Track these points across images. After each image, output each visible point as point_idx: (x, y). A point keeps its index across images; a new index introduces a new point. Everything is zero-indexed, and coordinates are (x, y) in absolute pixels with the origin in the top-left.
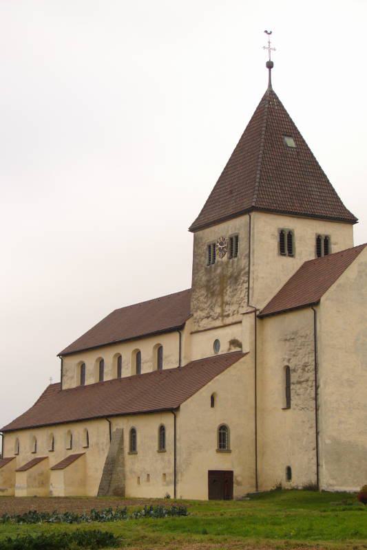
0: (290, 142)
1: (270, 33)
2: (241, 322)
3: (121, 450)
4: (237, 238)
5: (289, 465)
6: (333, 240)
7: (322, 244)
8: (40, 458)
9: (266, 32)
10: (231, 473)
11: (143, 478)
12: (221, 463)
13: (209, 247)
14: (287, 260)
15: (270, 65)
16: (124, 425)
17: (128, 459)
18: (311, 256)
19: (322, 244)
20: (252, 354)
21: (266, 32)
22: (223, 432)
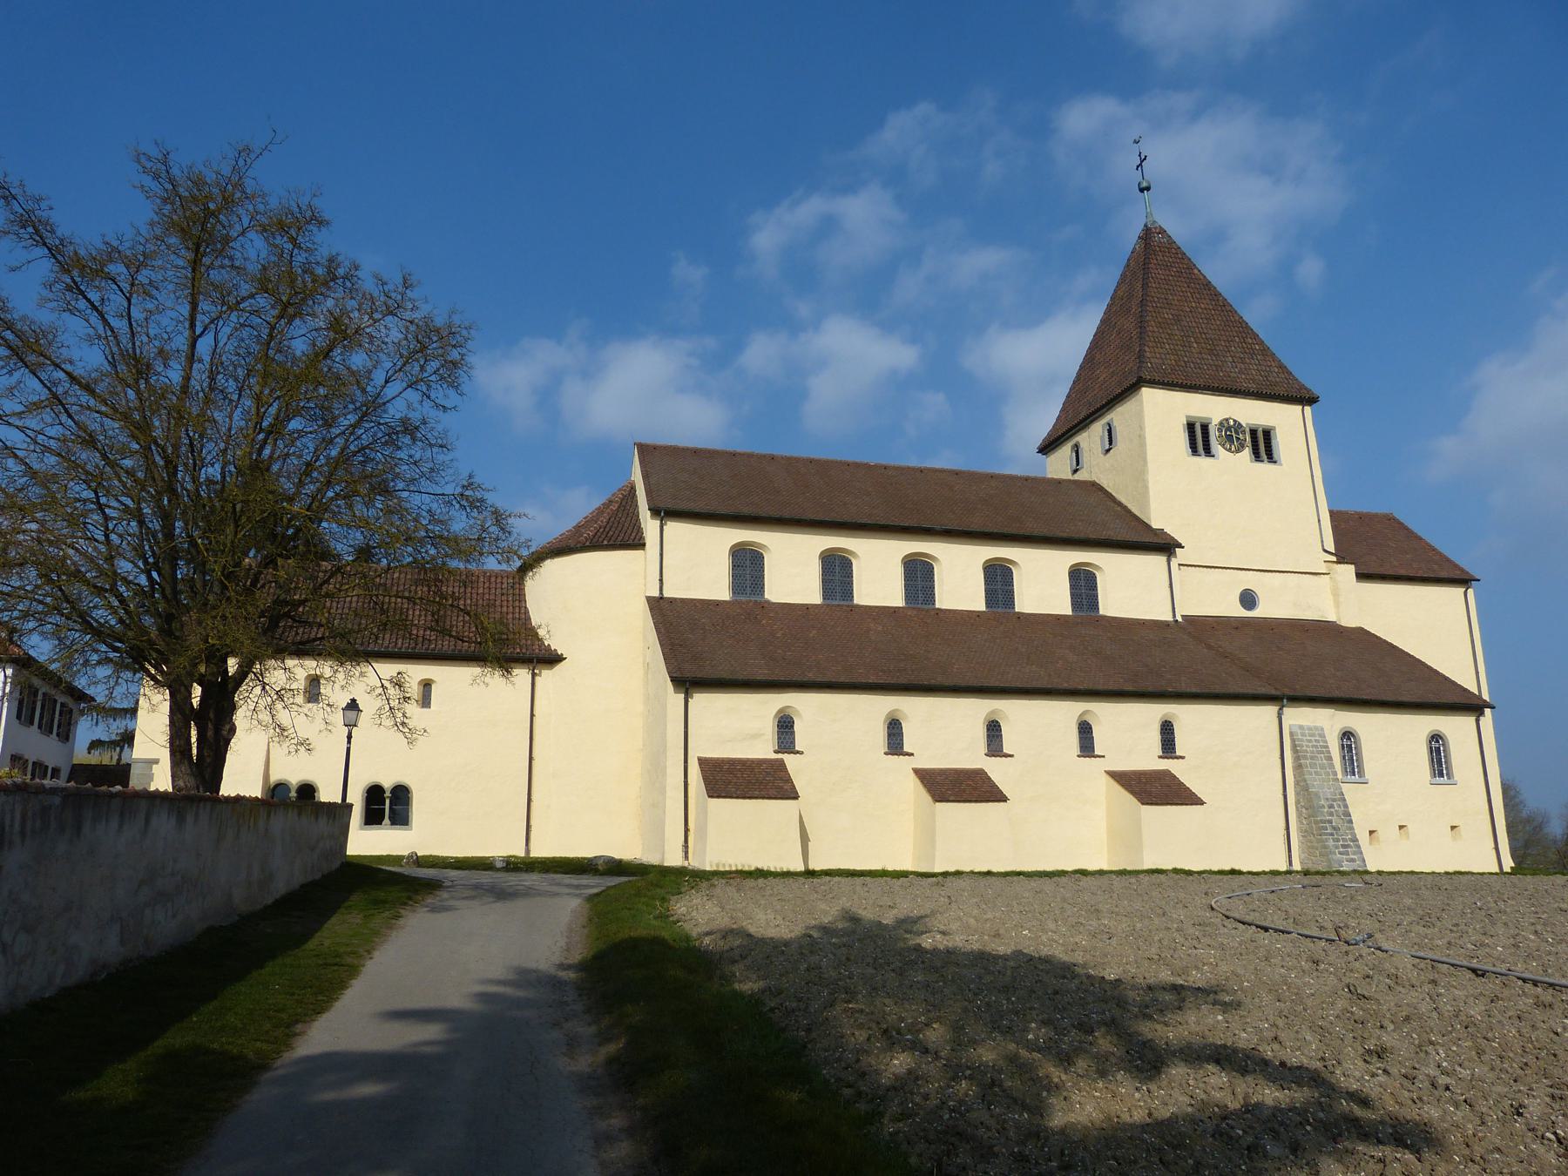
4: (1267, 434)
13: (1190, 427)
16: (1328, 722)
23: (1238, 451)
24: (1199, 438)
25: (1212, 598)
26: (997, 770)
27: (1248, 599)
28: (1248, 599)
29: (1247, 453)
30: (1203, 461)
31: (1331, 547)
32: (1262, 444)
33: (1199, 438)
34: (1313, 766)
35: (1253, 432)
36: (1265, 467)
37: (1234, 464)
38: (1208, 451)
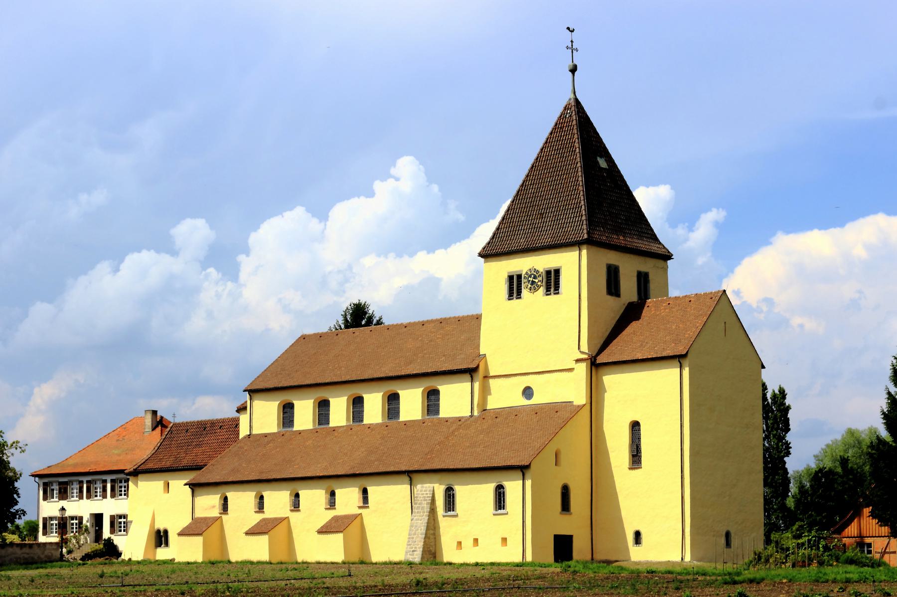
0: (603, 163)
1: (572, 31)
2: (571, 370)
3: (433, 510)
4: (557, 272)
5: (637, 529)
6: (651, 277)
7: (643, 280)
8: (276, 519)
9: (568, 28)
10: (570, 538)
11: (468, 543)
12: (565, 525)
13: (511, 278)
14: (611, 299)
15: (573, 70)
17: (445, 524)
18: (634, 298)
19: (643, 280)
20: (588, 406)
21: (568, 28)
22: (565, 492)
23: (536, 290)
24: (515, 287)
25: (504, 396)
26: (294, 517)
27: (528, 392)
28: (528, 392)
29: (542, 290)
30: (515, 302)
31: (585, 347)
32: (552, 281)
33: (515, 287)
34: (423, 508)
35: (548, 273)
36: (553, 297)
37: (534, 299)
38: (519, 296)
